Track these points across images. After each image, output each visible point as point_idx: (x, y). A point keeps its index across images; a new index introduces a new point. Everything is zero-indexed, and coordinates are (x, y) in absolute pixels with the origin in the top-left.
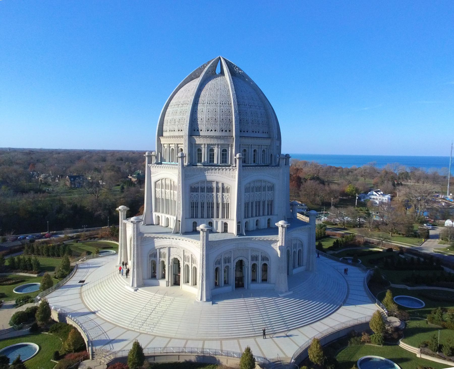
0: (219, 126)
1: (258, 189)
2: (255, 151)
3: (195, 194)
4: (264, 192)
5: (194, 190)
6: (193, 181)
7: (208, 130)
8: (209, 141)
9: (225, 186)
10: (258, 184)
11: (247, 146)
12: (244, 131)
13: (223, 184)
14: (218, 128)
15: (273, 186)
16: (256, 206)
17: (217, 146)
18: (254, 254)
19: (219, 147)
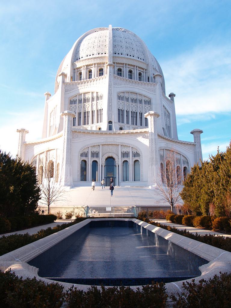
0: (96, 50)
1: (134, 101)
2: (130, 72)
3: (73, 105)
4: (141, 105)
5: (72, 102)
6: (72, 94)
7: (87, 56)
8: (88, 63)
9: (99, 95)
10: (134, 97)
11: (122, 65)
12: (118, 54)
13: (97, 93)
14: (95, 53)
15: (150, 101)
16: (132, 117)
17: (94, 65)
18: (125, 150)
19: (96, 65)
